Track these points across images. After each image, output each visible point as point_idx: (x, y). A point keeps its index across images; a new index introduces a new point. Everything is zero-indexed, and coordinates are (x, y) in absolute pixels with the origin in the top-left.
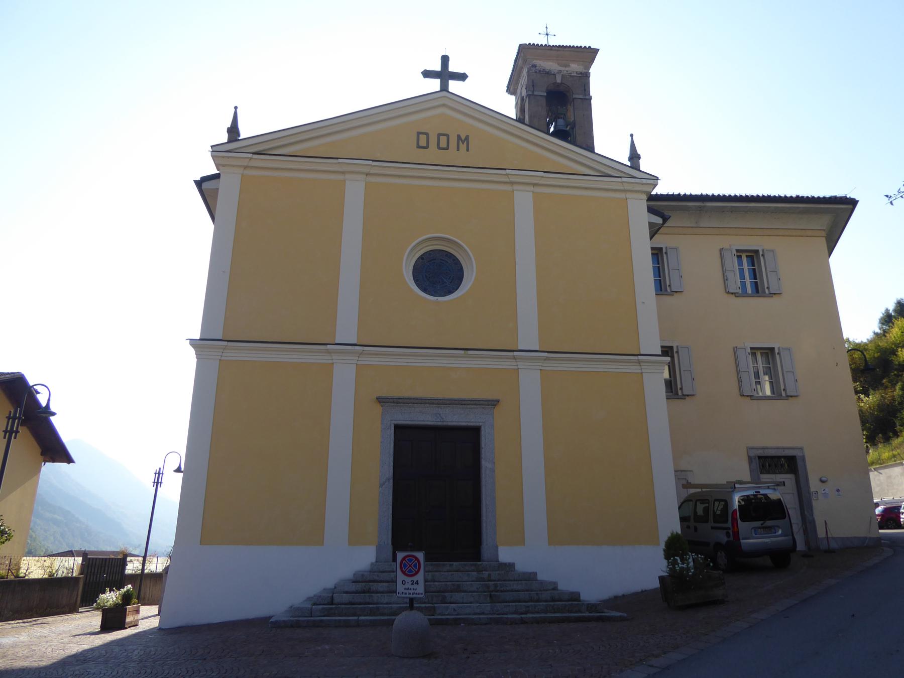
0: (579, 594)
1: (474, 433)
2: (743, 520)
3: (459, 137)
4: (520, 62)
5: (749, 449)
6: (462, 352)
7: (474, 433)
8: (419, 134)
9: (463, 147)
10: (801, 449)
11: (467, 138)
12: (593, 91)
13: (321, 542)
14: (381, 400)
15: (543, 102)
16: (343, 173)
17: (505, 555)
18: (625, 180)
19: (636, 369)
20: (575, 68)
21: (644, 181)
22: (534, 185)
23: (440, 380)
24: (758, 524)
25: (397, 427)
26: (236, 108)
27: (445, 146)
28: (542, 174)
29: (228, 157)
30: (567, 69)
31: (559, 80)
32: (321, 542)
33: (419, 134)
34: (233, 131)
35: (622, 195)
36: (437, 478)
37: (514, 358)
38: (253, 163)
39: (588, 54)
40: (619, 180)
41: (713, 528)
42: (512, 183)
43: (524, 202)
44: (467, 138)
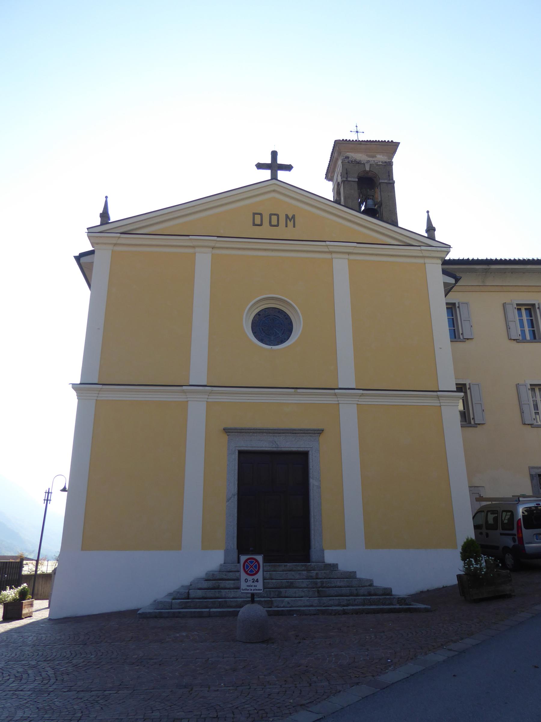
0: (391, 590)
1: (302, 458)
2: (526, 528)
3: (287, 216)
4: (336, 155)
5: (531, 468)
6: (293, 390)
7: (302, 458)
8: (254, 214)
9: (290, 224)
11: (294, 217)
12: (395, 178)
13: (179, 547)
14: (227, 431)
15: (356, 186)
16: (194, 247)
17: (330, 557)
18: (423, 248)
19: (436, 403)
20: (381, 158)
21: (439, 249)
22: (349, 253)
23: (276, 414)
25: (240, 453)
26: (106, 197)
27: (276, 223)
28: (355, 244)
29: (101, 237)
30: (374, 159)
31: (367, 168)
32: (179, 547)
34: (105, 215)
35: (421, 261)
36: (273, 495)
37: (335, 394)
38: (120, 241)
39: (391, 147)
40: (419, 248)
41: (501, 534)
42: (331, 252)
43: (341, 267)
44: (294, 217)
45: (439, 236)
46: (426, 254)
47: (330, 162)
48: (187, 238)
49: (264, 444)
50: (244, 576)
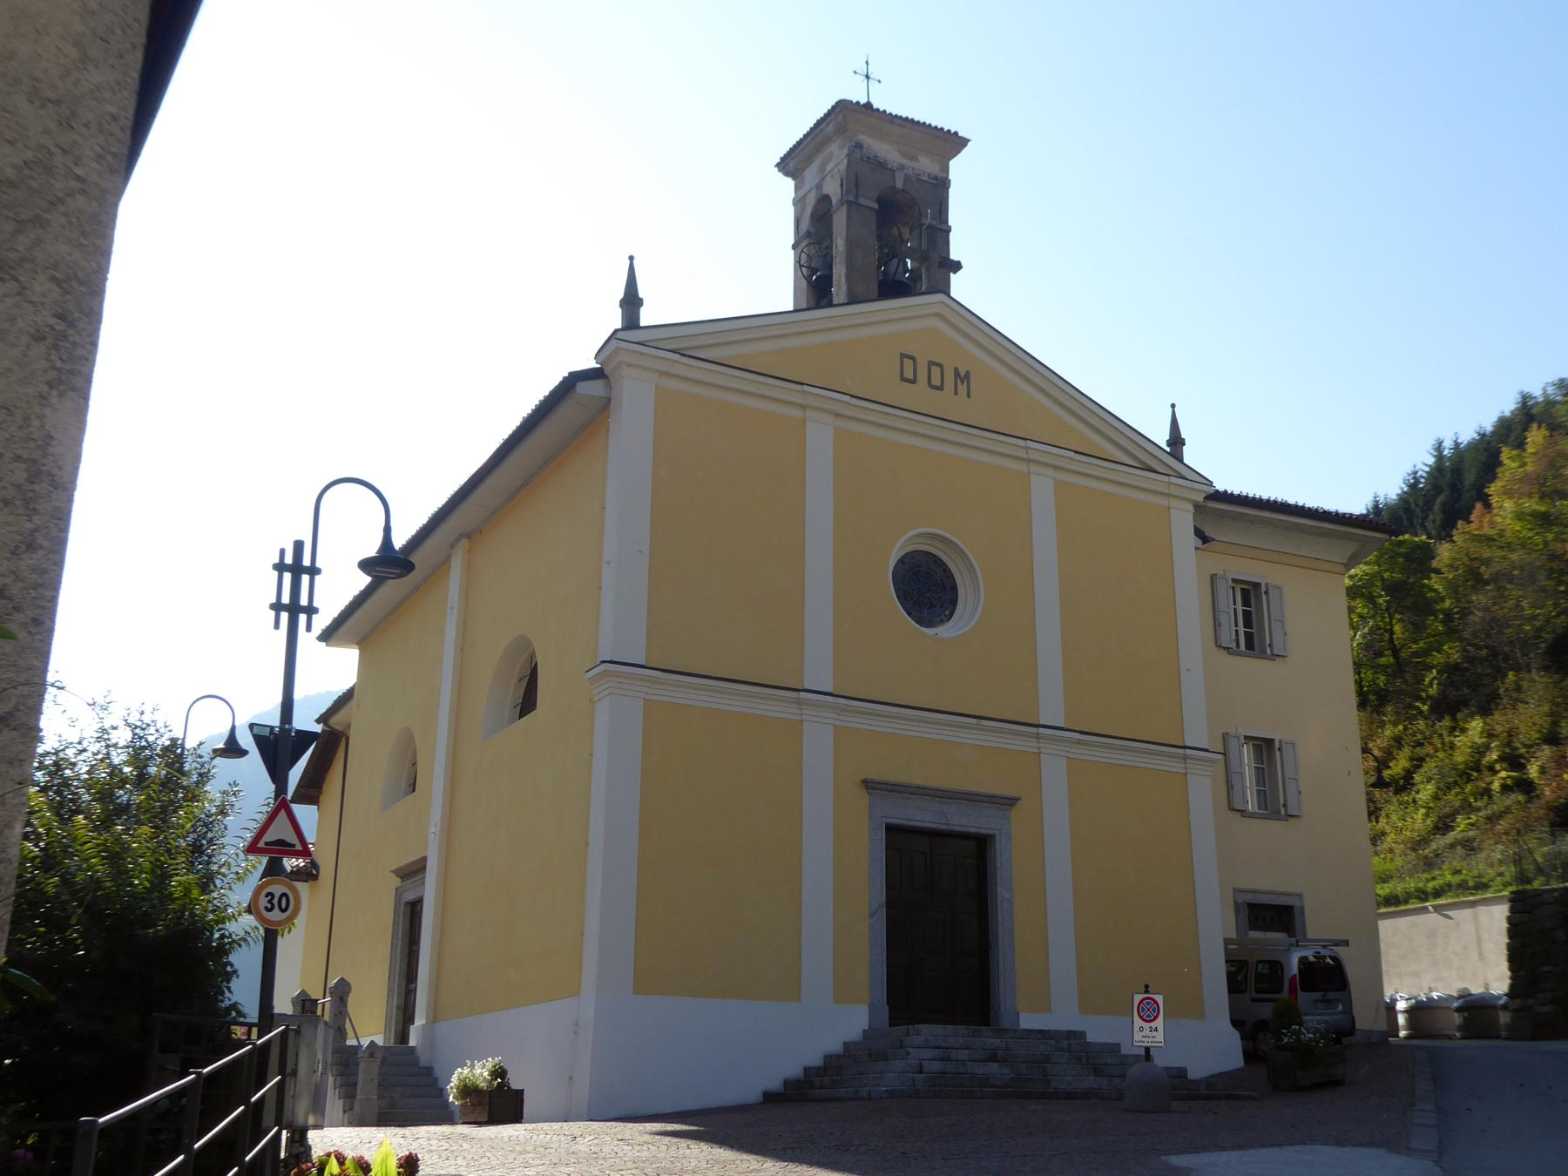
1: (982, 844)
2: (1304, 989)
3: (956, 370)
4: (830, 128)
5: (1236, 891)
7: (982, 844)
8: (903, 356)
9: (962, 388)
10: (1300, 896)
11: (968, 373)
12: (954, 218)
14: (868, 785)
16: (803, 407)
17: (1028, 1021)
18: (1174, 480)
19: (1178, 767)
20: (926, 164)
21: (1196, 486)
22: (1055, 468)
23: (948, 762)
24: (1318, 995)
25: (891, 830)
29: (641, 354)
30: (913, 164)
31: (899, 184)
33: (903, 356)
34: (631, 302)
35: (1163, 501)
37: (1037, 736)
39: (953, 143)
40: (1166, 479)
41: (1253, 1000)
42: (1029, 461)
43: (1042, 488)
44: (968, 373)
45: (1190, 456)
46: (1174, 491)
47: (805, 136)
48: (798, 387)
49: (924, 816)
50: (1138, 1022)
